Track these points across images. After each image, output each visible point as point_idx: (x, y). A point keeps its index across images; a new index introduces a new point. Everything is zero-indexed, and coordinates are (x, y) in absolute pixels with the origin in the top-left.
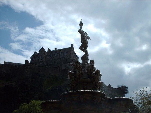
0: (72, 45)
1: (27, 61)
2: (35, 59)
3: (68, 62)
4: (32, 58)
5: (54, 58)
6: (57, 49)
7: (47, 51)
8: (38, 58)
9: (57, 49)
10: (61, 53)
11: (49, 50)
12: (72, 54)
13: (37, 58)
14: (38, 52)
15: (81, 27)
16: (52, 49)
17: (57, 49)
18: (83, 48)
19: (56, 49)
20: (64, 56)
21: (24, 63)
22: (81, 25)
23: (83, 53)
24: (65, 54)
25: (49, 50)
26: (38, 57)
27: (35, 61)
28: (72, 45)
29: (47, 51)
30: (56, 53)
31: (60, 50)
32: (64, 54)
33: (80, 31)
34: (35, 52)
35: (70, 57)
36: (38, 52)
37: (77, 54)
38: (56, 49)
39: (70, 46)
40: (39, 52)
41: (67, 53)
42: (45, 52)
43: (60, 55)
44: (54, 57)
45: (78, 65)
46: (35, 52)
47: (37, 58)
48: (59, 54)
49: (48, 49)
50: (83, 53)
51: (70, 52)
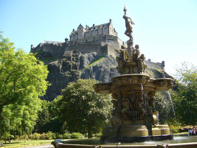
0: (110, 20)
1: (66, 40)
4: (70, 37)
6: (96, 25)
10: (99, 30)
13: (76, 35)
15: (125, 14)
16: (91, 26)
18: (128, 33)
19: (94, 25)
21: (64, 41)
22: (125, 10)
23: (128, 38)
24: (104, 30)
26: (77, 34)
30: (94, 30)
31: (99, 27)
33: (125, 18)
34: (74, 30)
35: (109, 33)
36: (76, 30)
39: (109, 22)
40: (78, 29)
42: (84, 29)
47: (76, 35)
49: (86, 25)
50: (128, 38)
51: (108, 27)
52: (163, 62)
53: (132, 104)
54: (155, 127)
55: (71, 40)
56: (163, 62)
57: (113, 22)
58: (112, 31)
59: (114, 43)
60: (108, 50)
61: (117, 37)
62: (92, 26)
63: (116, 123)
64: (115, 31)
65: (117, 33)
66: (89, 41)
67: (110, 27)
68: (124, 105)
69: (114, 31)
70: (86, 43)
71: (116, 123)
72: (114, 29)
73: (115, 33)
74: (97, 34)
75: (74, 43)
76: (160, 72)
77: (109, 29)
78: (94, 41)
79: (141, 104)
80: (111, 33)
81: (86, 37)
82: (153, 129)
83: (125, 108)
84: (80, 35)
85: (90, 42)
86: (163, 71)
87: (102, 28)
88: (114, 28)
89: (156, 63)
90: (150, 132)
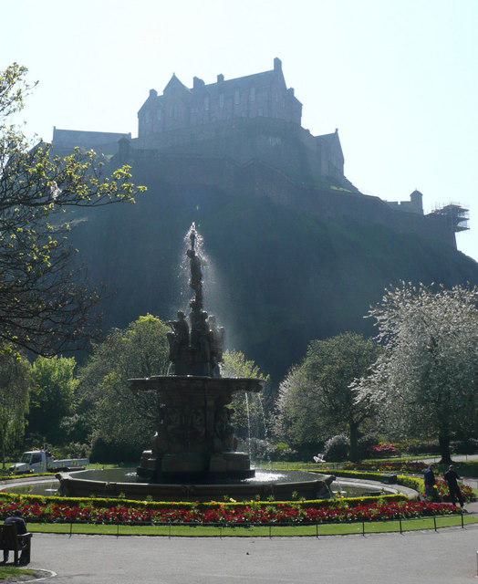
0: (278, 63)
4: (141, 114)
7: (189, 85)
9: (226, 79)
11: (197, 82)
14: (160, 93)
17: (226, 79)
19: (220, 77)
25: (197, 82)
28: (278, 63)
29: (189, 85)
34: (153, 92)
36: (160, 93)
38: (220, 77)
39: (270, 67)
46: (153, 92)
57: (285, 69)
62: (215, 81)
88: (288, 87)
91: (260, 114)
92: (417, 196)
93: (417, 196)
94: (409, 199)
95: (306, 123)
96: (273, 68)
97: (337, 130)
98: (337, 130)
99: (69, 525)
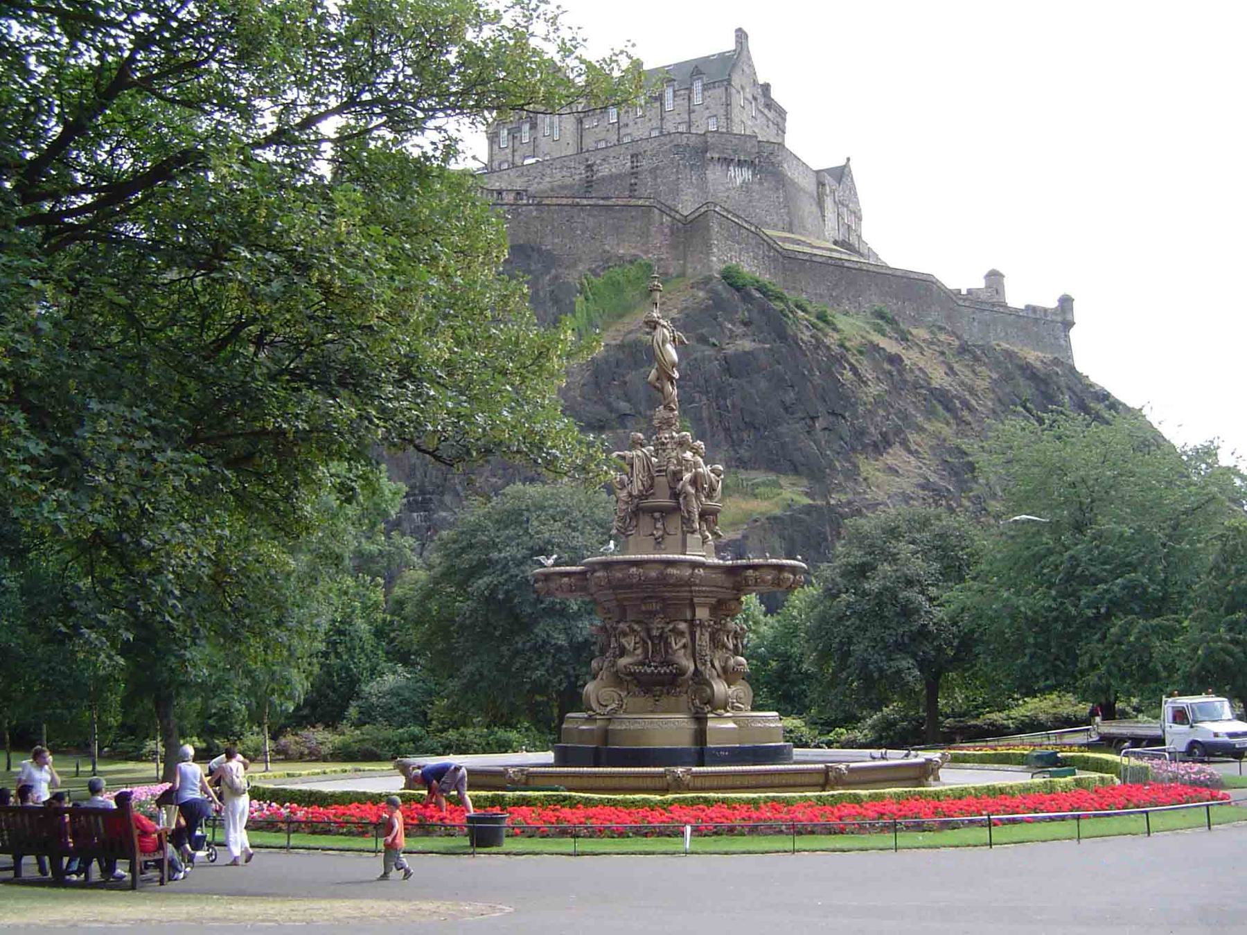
0: (741, 35)
2: (514, 138)
3: (716, 156)
5: (627, 125)
8: (531, 128)
9: (646, 67)
10: (669, 94)
12: (738, 100)
13: (526, 127)
17: (646, 67)
20: (690, 112)
24: (697, 99)
27: (514, 151)
28: (741, 35)
31: (668, 76)
32: (689, 99)
35: (728, 118)
37: (775, 94)
39: (729, 45)
41: (706, 93)
43: (669, 106)
44: (631, 124)
45: (638, 456)
48: (660, 98)
52: (1066, 303)
53: (652, 642)
54: (720, 717)
55: (499, 157)
56: (1066, 303)
57: (753, 45)
58: (748, 107)
59: (756, 187)
60: (715, 250)
61: (781, 145)
63: (599, 702)
64: (770, 104)
65: (782, 113)
66: (604, 171)
67: (736, 80)
68: (626, 645)
69: (761, 100)
70: (589, 184)
71: (599, 702)
72: (766, 88)
73: (771, 115)
74: (655, 123)
75: (509, 198)
76: (1038, 364)
77: (728, 95)
78: (634, 174)
79: (680, 644)
80: (746, 121)
81: (589, 143)
82: (710, 724)
83: (632, 653)
84: (552, 128)
85: (612, 178)
86: (1056, 362)
87: (690, 89)
88: (761, 82)
89: (1023, 307)
90: (700, 735)
91: (712, 128)
92: (994, 278)
93: (994, 278)
94: (981, 284)
95: (794, 141)
96: (733, 47)
97: (848, 159)
98: (848, 159)
99: (791, 837)
